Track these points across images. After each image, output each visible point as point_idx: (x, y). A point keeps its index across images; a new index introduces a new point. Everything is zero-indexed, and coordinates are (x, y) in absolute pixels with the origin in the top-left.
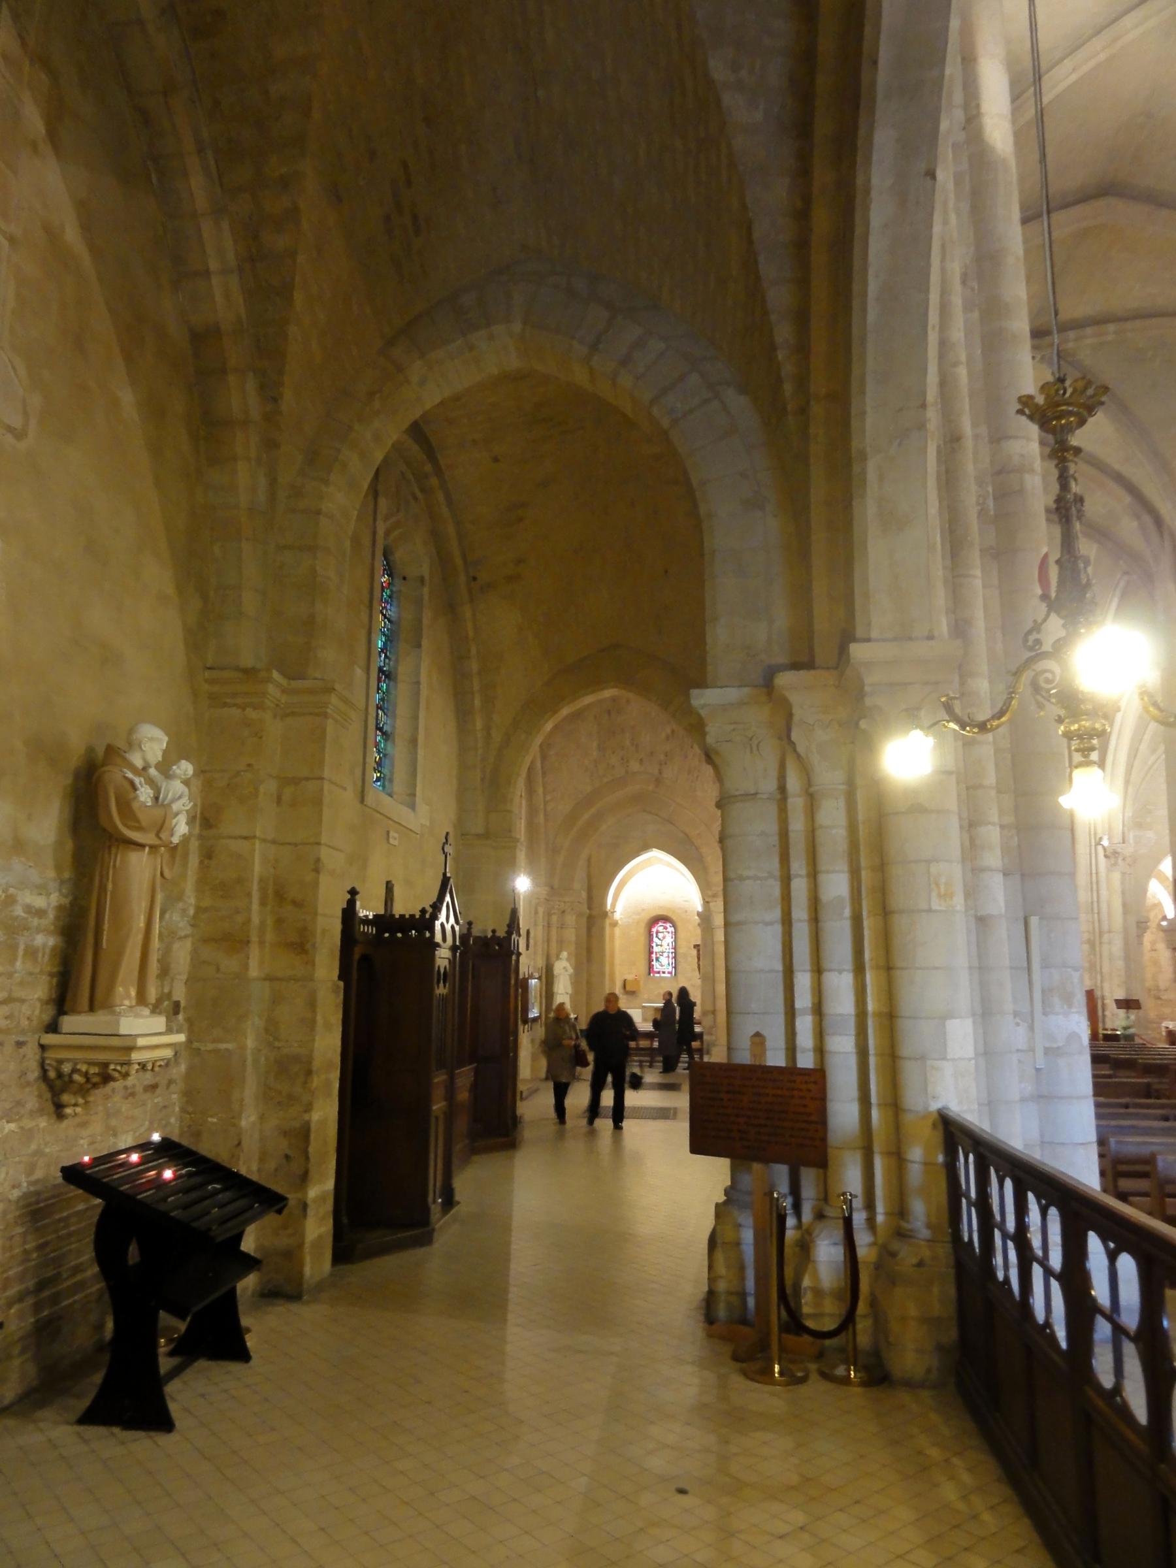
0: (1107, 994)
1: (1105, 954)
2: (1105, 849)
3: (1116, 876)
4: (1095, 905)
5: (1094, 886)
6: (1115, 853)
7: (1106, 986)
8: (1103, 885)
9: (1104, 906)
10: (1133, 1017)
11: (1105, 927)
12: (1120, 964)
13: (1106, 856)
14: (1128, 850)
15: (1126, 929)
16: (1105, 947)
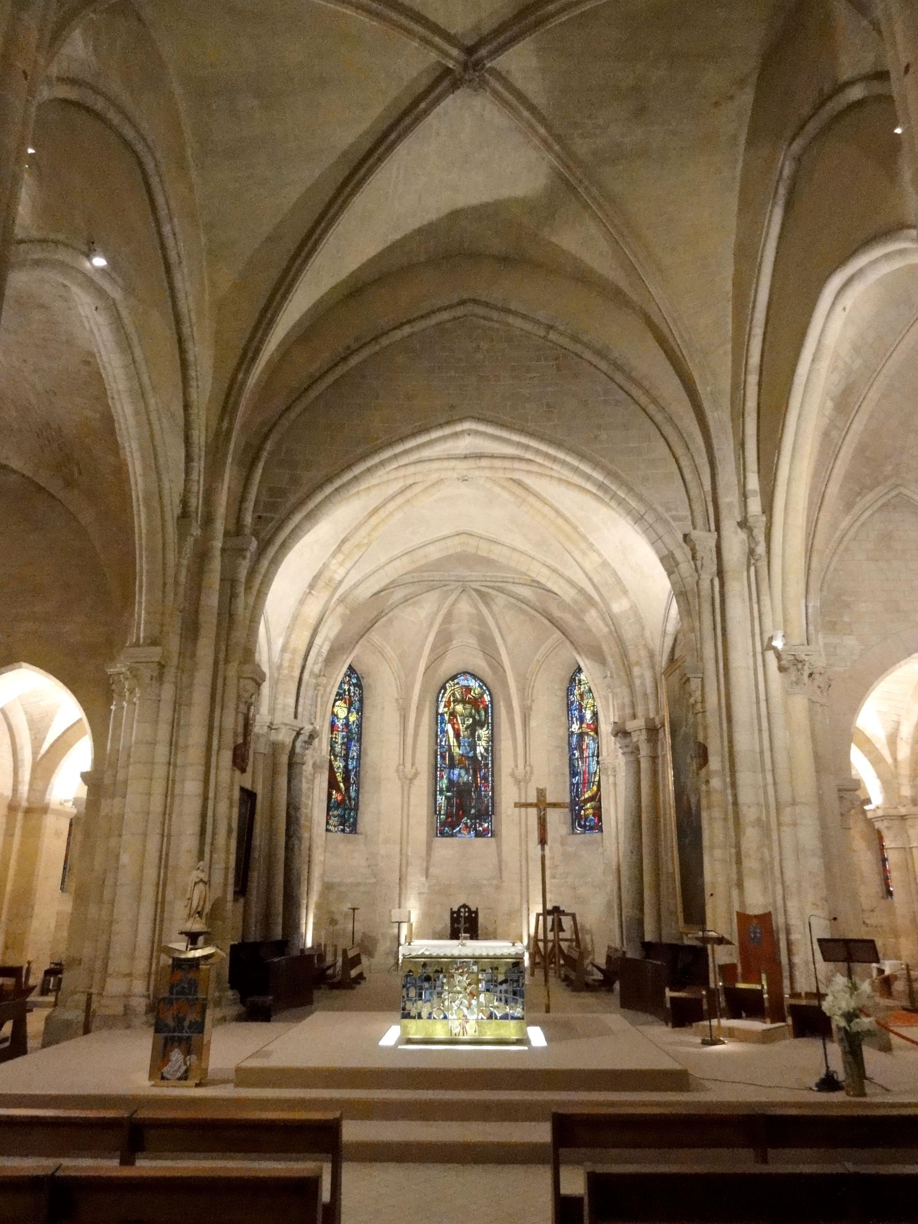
0: (794, 921)
1: (788, 843)
2: (779, 657)
3: (799, 703)
4: (767, 754)
5: (765, 721)
6: (797, 661)
7: (792, 905)
8: (779, 721)
9: (781, 757)
10: (865, 987)
11: (785, 795)
12: (814, 863)
13: (782, 669)
14: (819, 661)
15: (820, 798)
16: (787, 831)
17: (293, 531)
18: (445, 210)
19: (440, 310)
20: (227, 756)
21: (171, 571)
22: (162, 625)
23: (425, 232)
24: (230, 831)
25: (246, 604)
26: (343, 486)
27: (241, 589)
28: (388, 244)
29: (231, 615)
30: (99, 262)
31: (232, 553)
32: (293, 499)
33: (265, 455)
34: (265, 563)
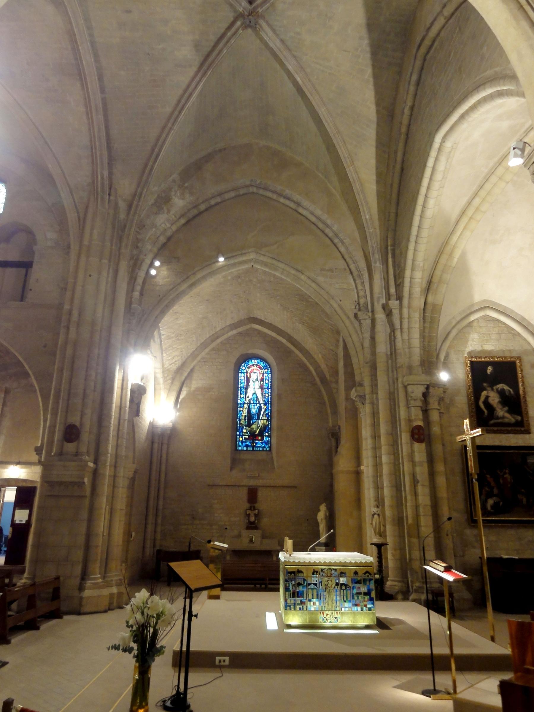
17: (411, 282)
18: (364, 32)
19: (411, 75)
20: (405, 437)
21: (358, 344)
22: (361, 373)
23: (376, 50)
24: (415, 482)
25: (402, 340)
26: (417, 236)
27: (398, 333)
28: (371, 80)
29: (395, 350)
30: (221, 259)
31: (389, 314)
32: (402, 265)
33: (389, 248)
34: (405, 311)
